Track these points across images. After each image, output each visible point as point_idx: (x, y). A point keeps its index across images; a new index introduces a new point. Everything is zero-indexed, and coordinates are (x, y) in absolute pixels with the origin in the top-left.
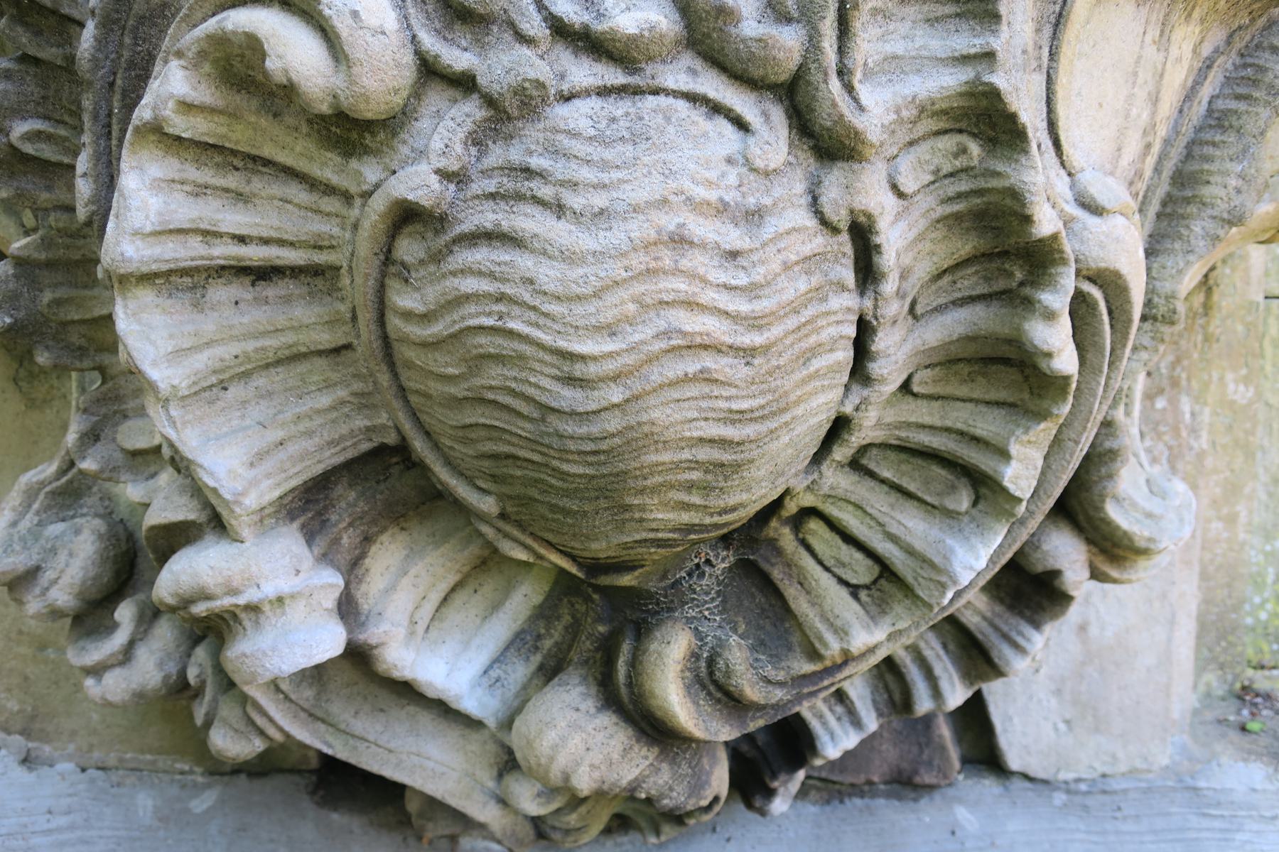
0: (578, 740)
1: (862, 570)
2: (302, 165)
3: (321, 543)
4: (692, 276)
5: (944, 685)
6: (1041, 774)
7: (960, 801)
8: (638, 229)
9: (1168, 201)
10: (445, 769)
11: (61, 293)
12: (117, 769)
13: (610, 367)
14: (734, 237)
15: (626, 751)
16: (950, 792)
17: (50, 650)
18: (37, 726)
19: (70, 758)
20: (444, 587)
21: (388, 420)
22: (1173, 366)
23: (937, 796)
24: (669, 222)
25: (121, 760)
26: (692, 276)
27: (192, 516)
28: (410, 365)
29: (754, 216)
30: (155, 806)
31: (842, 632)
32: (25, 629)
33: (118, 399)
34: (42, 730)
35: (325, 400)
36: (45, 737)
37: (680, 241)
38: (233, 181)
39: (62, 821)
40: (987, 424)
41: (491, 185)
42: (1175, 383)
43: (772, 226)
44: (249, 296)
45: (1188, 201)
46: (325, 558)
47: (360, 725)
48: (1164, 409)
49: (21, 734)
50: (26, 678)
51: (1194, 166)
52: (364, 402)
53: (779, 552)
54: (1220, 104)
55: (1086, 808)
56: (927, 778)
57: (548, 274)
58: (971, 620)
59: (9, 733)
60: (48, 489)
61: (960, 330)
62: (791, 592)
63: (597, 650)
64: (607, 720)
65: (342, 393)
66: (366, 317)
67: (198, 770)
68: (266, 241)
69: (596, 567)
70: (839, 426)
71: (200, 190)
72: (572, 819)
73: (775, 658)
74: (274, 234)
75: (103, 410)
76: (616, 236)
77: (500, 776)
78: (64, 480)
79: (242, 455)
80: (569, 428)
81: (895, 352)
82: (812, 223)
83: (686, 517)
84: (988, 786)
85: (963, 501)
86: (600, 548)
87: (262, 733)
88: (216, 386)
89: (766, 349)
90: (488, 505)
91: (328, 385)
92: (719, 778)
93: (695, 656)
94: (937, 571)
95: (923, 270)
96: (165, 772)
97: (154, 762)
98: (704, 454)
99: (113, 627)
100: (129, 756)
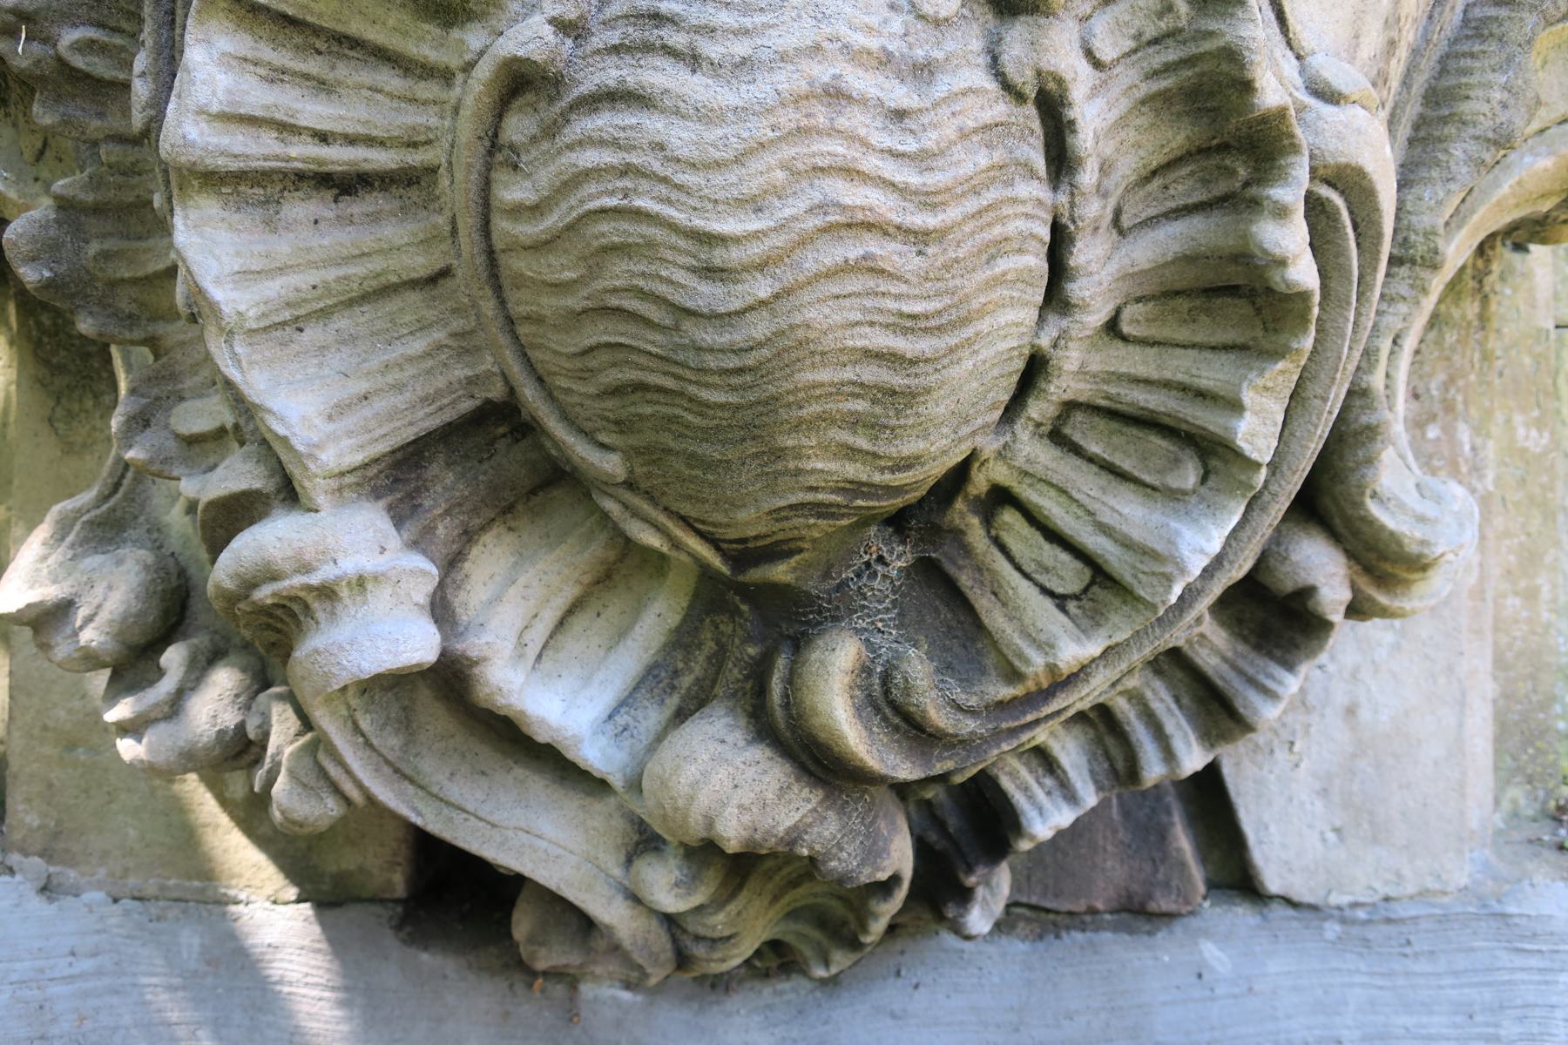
0: (727, 781)
1: (1070, 577)
2: (394, 42)
3: (411, 529)
4: (852, 138)
5: (1178, 744)
6: (1306, 897)
7: (1206, 933)
8: (787, 80)
9: (1420, 123)
10: (560, 851)
11: (111, 244)
12: (157, 898)
13: (755, 250)
14: (900, 95)
15: (783, 791)
16: (1194, 922)
17: (81, 750)
18: (61, 845)
19: (99, 886)
20: (560, 603)
21: (496, 364)
22: (1446, 387)
23: (1178, 927)
24: (822, 72)
25: (163, 888)
26: (852, 138)
27: (257, 485)
28: (520, 282)
29: (923, 71)
30: (202, 946)
31: (1046, 646)
32: (51, 724)
33: (174, 377)
34: (67, 851)
35: (418, 345)
36: (70, 860)
37: (836, 95)
38: (314, 66)
39: (87, 965)
40: (1211, 373)
41: (614, 38)
42: (1449, 407)
43: (944, 85)
44: (331, 215)
45: (1444, 120)
46: (414, 545)
47: (454, 791)
48: (1438, 439)
49: (41, 855)
50: (50, 786)
51: (1450, 81)
52: (465, 345)
53: (967, 550)
54: (1477, 12)
55: (1366, 942)
56: (1163, 903)
57: (681, 136)
58: (1208, 661)
59: (26, 855)
60: (85, 518)
61: (1175, 248)
62: (983, 603)
63: (747, 678)
64: (760, 753)
65: (439, 335)
66: (468, 224)
68: (351, 140)
69: (745, 554)
70: (1035, 370)
71: (278, 75)
72: (718, 922)
73: (966, 683)
74: (362, 130)
75: (155, 391)
76: (761, 89)
77: (629, 861)
78: (105, 507)
79: (319, 406)
80: (709, 336)
81: (1100, 269)
82: (992, 86)
83: (854, 470)
84: (1241, 915)
85: (1188, 476)
86: (749, 521)
87: (336, 790)
88: (289, 323)
89: (940, 234)
90: (611, 465)
91: (423, 327)
92: (900, 856)
93: (866, 670)
94: (1158, 559)
95: (1127, 167)
98: (871, 373)
99: (161, 673)
100: (172, 882)
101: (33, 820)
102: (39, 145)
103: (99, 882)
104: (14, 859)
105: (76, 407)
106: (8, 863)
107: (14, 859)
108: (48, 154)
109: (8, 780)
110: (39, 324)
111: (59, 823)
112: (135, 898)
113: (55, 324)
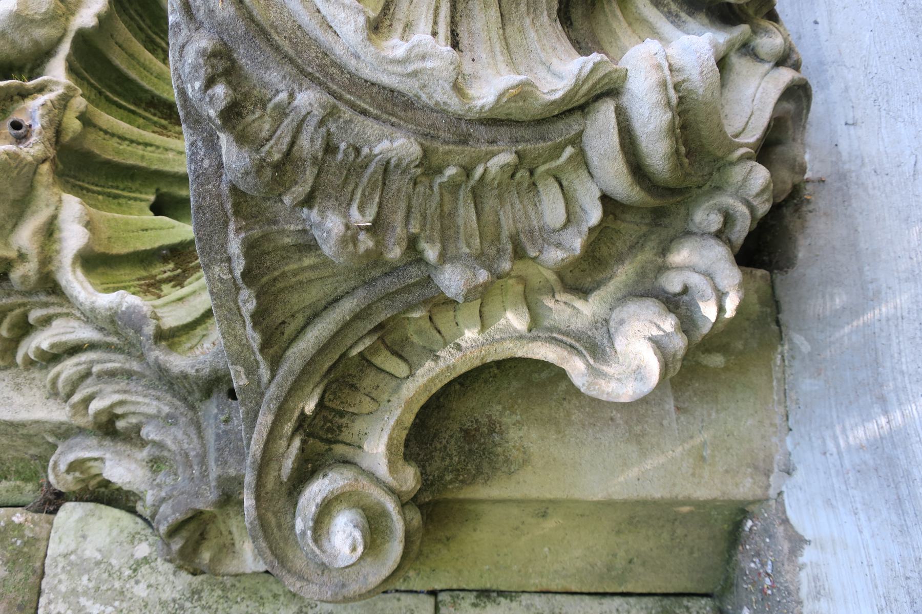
10: (760, 89)
12: (786, 407)
17: (705, 454)
18: (761, 464)
19: (782, 440)
25: (779, 403)
27: (612, 108)
32: (691, 471)
34: (764, 460)
35: (532, 34)
36: (769, 459)
44: (469, 55)
49: (769, 477)
50: (727, 471)
59: (769, 486)
60: (591, 361)
67: (779, 350)
68: (435, 23)
74: (432, 11)
75: (540, 241)
78: (585, 352)
91: (522, 30)
96: (784, 373)
97: (778, 380)
100: (776, 398)
101: (748, 482)
102: (368, 399)
103: (780, 441)
104: (772, 493)
105: (501, 458)
106: (775, 496)
107: (772, 493)
108: (373, 395)
109: (726, 498)
110: (451, 482)
111: (748, 466)
112: (787, 419)
113: (452, 472)
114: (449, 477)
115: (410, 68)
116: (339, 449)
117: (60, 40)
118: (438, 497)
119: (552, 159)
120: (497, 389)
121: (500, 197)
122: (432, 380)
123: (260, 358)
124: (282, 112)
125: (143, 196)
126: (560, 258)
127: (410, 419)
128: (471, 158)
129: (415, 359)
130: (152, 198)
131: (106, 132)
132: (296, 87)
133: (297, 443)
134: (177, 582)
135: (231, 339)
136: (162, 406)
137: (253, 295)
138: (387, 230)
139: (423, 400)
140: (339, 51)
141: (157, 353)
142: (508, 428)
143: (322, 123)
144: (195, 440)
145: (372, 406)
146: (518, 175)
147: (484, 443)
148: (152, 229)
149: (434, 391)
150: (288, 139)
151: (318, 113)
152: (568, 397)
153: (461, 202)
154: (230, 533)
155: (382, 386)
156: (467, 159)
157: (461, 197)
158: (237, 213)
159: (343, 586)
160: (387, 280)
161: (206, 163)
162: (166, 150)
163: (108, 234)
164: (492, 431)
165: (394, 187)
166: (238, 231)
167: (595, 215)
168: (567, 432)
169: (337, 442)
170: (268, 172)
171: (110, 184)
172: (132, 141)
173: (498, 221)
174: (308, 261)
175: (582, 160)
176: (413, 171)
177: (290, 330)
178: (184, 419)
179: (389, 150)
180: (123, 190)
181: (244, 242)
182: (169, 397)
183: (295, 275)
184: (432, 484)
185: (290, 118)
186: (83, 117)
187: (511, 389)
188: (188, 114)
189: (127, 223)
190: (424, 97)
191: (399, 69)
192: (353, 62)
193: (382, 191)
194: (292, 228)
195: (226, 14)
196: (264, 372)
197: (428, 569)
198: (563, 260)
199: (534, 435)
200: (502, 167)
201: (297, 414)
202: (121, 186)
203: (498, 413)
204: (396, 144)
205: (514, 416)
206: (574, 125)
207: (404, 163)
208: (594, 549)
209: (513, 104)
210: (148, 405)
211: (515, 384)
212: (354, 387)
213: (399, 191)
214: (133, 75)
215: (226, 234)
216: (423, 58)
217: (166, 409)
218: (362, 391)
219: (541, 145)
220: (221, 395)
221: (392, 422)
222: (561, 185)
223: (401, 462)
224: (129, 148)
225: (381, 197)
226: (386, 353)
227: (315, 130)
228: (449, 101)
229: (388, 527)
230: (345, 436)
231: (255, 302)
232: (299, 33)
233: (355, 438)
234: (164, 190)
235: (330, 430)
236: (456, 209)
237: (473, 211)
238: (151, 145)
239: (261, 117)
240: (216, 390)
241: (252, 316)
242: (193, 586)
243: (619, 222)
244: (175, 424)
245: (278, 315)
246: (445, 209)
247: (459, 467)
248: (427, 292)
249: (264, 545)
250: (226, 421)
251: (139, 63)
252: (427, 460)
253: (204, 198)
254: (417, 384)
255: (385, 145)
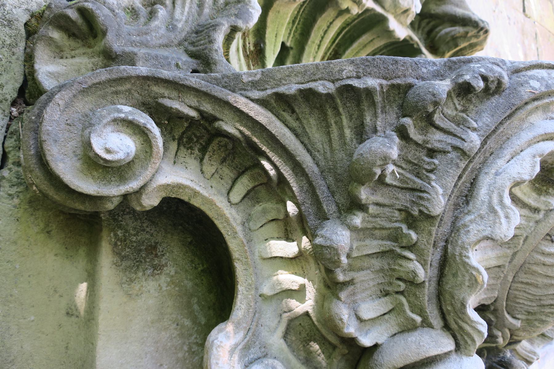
102: (214, 171)
105: (133, 276)
108: (216, 175)
110: (116, 235)
113: (124, 236)
114: (120, 233)
115: (498, 208)
116: (174, 146)
117: (383, 7)
118: (104, 224)
119: (410, 307)
120: (186, 271)
121: (382, 270)
122: (227, 221)
123: (269, 92)
124: (461, 122)
125: (290, 39)
126: (343, 317)
127: (196, 202)
128: (423, 250)
129: (242, 208)
130: (288, 44)
131: (331, 23)
132: (482, 132)
133: (193, 114)
134: (20, 10)
135: (287, 73)
136: (182, 23)
137: (330, 91)
138: (372, 189)
139: (211, 214)
140: (500, 163)
141: (226, 26)
142: (156, 280)
143: (456, 148)
144: (160, 42)
145: (208, 175)
146: (401, 283)
147: (146, 262)
148: (276, 40)
149: (216, 222)
150: (442, 125)
151: (466, 146)
152: (179, 327)
153: (381, 242)
154: (73, 57)
155: (222, 181)
156: (423, 247)
157: (384, 242)
158: (393, 86)
159: (56, 141)
160: (325, 189)
161: (424, 70)
162: (314, 57)
163: (281, 11)
164: (155, 267)
165: (400, 195)
166: (381, 86)
167: (366, 341)
168: (152, 329)
169: (179, 145)
170: (431, 109)
171: (302, 20)
172: (322, 38)
173: (362, 269)
174: (348, 132)
175: (409, 328)
176: (416, 209)
177: (287, 116)
178: (173, 37)
179: (437, 193)
180: (296, 27)
181: (375, 88)
182: (187, 29)
183: (336, 123)
184: (115, 220)
185: (456, 127)
186: (347, 10)
187: (186, 282)
188: (455, 63)
189: (282, 25)
190: (468, 218)
191: (495, 200)
192: (493, 171)
193: (399, 187)
194: (378, 123)
195: (523, 93)
196: (256, 94)
197: (19, 215)
198: (341, 319)
199: (151, 302)
200: (414, 272)
201: (218, 115)
202: (299, 27)
203: (168, 272)
204: (440, 197)
205: (165, 285)
206: (437, 322)
207: (425, 203)
208: (30, 362)
209: (467, 278)
210: (182, 13)
211: (189, 284)
212: (223, 161)
213: (397, 199)
214: (355, 45)
215: (379, 78)
216: (507, 217)
217: (180, 25)
218: (220, 167)
219: (426, 298)
220: (195, 65)
221: (198, 188)
222: (385, 314)
223: (164, 195)
224: (319, 36)
225: (395, 186)
226: (251, 185)
227: (449, 144)
228: (472, 234)
229: (110, 182)
230: (183, 151)
231: (325, 92)
232: (505, 138)
233: (182, 160)
234: (291, 52)
235: (190, 140)
236: (376, 239)
237: (374, 251)
238: (318, 49)
239: (456, 109)
240: (199, 62)
241: (310, 89)
242: (16, 22)
243: (339, 358)
244: (168, 29)
245: (302, 109)
246: (377, 231)
247: (128, 241)
248: (312, 217)
249: (103, 78)
250: (177, 65)
251: (361, 49)
252: (134, 216)
253: (403, 66)
254: (225, 209)
255: (440, 191)
